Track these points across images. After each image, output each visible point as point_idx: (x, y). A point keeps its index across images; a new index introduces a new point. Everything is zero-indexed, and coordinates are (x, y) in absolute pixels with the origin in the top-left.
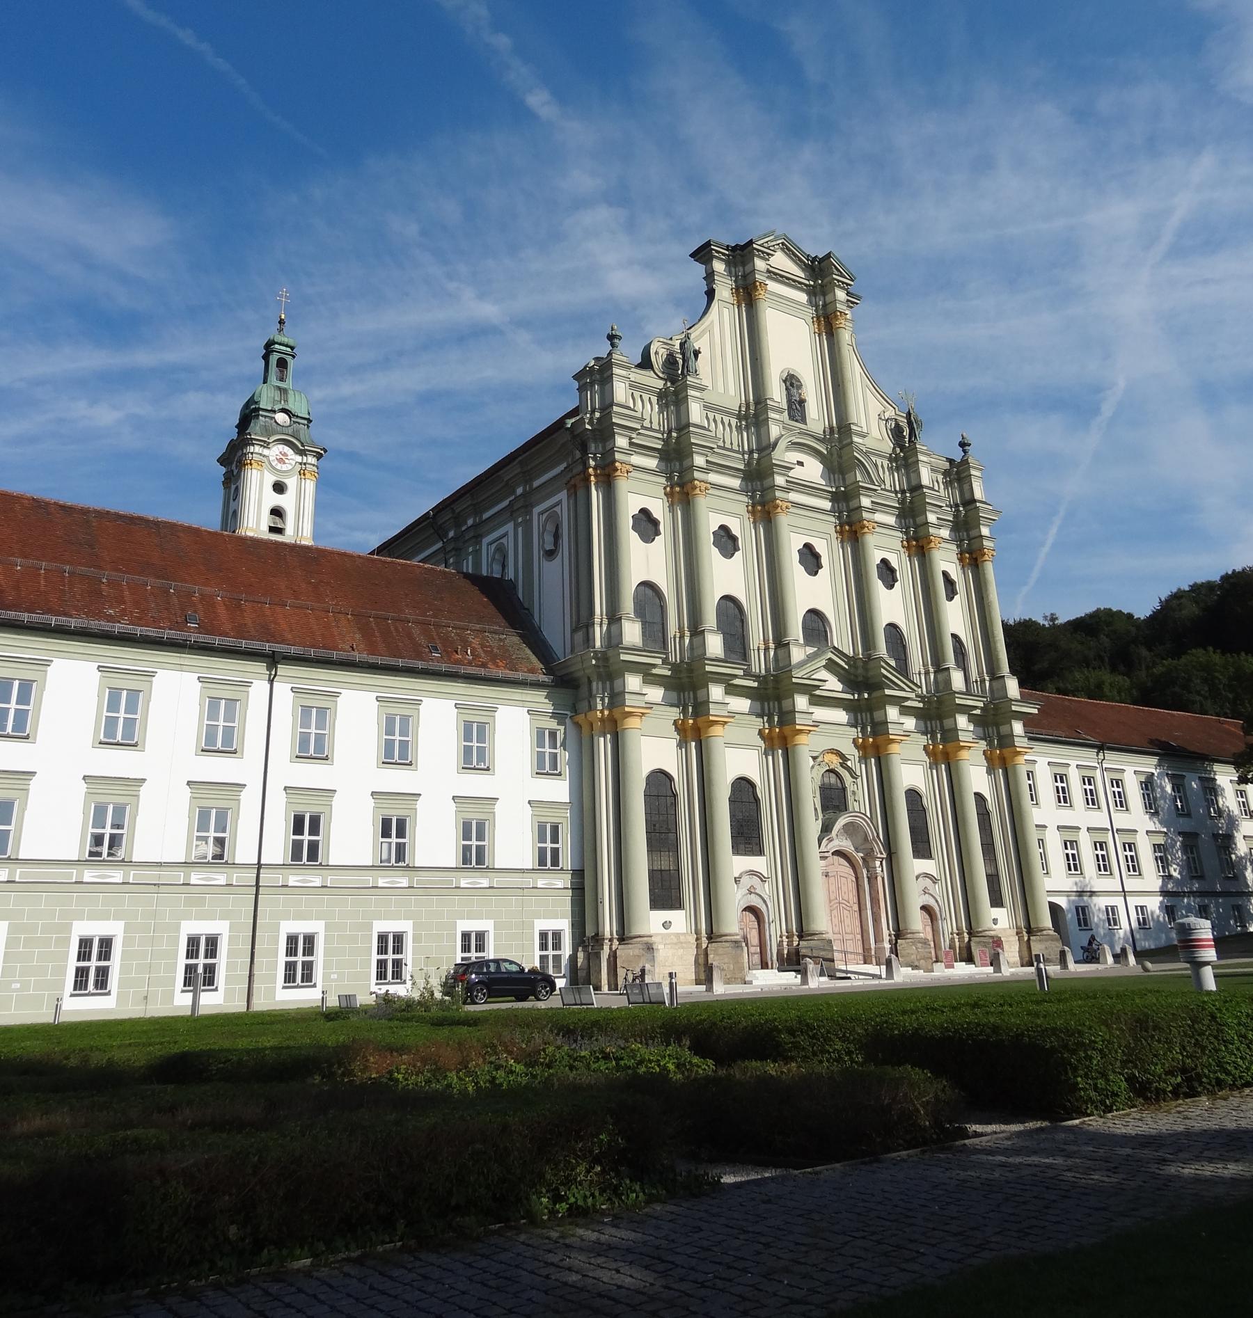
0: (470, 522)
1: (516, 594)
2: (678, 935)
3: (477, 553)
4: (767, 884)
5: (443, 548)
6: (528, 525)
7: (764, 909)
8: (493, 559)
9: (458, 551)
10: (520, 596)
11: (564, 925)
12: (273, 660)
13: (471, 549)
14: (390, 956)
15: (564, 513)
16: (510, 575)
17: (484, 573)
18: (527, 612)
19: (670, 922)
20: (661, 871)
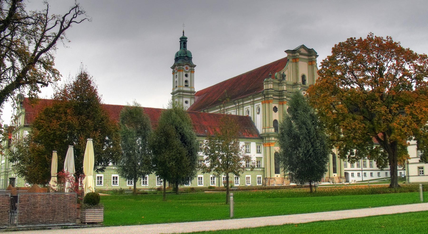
0: (241, 103)
1: (251, 120)
2: (279, 178)
3: (243, 109)
5: (236, 107)
6: (253, 107)
8: (247, 112)
9: (239, 108)
10: (252, 120)
11: (261, 176)
13: (242, 109)
16: (250, 115)
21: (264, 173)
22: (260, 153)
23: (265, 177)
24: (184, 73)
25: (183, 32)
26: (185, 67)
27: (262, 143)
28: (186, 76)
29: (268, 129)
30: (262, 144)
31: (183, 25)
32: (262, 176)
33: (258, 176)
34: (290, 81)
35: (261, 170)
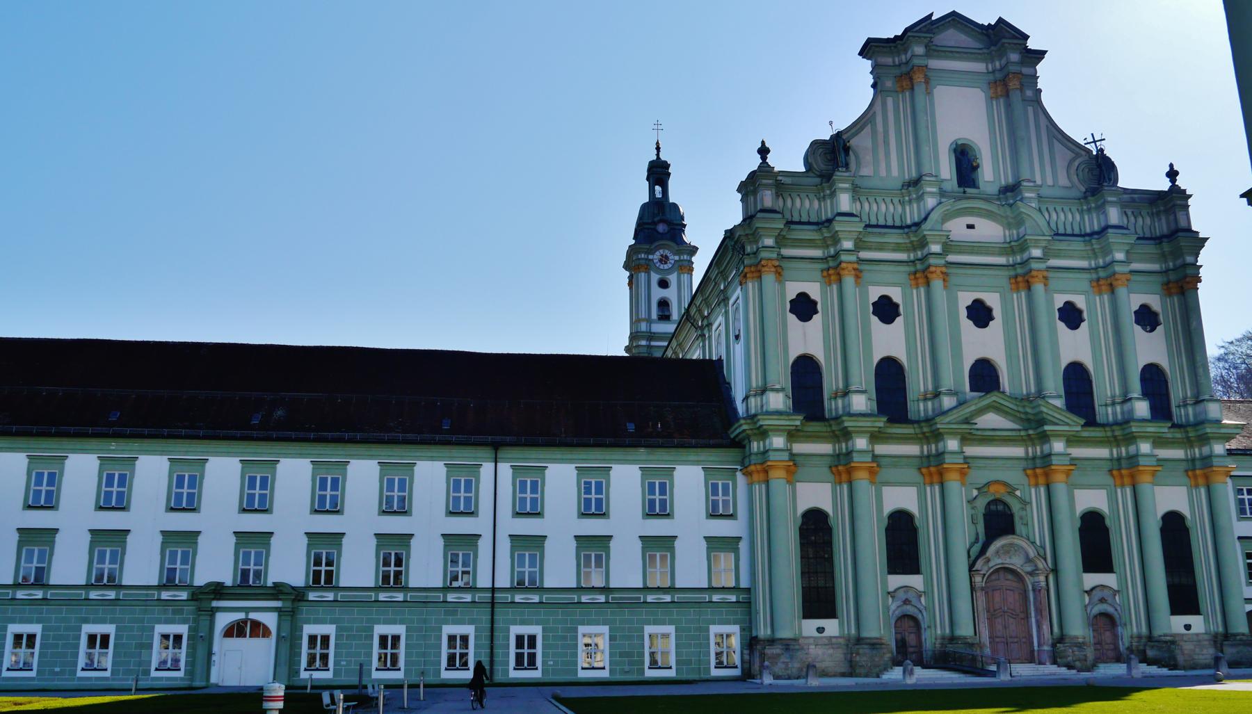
7: (920, 617)
12: (496, 446)
14: (526, 651)
15: (740, 301)
17: (707, 358)
18: (727, 385)
21: (750, 613)
22: (732, 516)
23: (754, 634)
24: (655, 277)
25: (658, 149)
26: (656, 257)
27: (739, 467)
28: (664, 284)
29: (759, 399)
30: (739, 474)
31: (656, 127)
32: (742, 630)
34: (883, 173)
35: (734, 600)
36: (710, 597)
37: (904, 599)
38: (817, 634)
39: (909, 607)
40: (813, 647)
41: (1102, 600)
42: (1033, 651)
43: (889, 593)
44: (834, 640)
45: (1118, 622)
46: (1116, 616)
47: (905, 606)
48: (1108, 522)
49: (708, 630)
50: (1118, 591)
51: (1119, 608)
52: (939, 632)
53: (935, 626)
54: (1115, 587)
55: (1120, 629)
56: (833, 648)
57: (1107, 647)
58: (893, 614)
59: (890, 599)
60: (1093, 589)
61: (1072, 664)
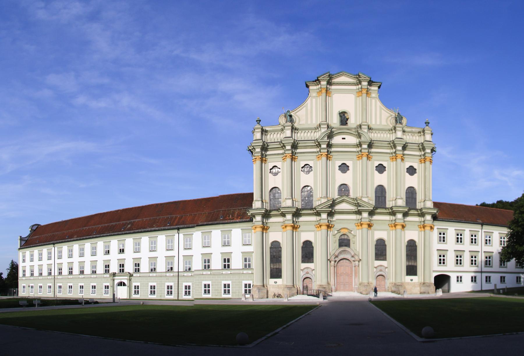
4: (313, 272)
7: (312, 278)
19: (276, 282)
20: (276, 268)
33: (244, 282)
34: (309, 122)
36: (243, 272)
37: (306, 272)
38: (274, 284)
39: (308, 275)
40: (272, 288)
41: (381, 271)
42: (353, 287)
43: (301, 270)
44: (279, 286)
45: (386, 278)
46: (385, 276)
47: (307, 274)
48: (386, 243)
49: (242, 282)
50: (387, 268)
51: (387, 274)
52: (318, 283)
53: (317, 281)
54: (386, 266)
55: (386, 280)
56: (279, 288)
57: (382, 286)
58: (302, 277)
59: (302, 272)
60: (378, 266)
61: (362, 292)
